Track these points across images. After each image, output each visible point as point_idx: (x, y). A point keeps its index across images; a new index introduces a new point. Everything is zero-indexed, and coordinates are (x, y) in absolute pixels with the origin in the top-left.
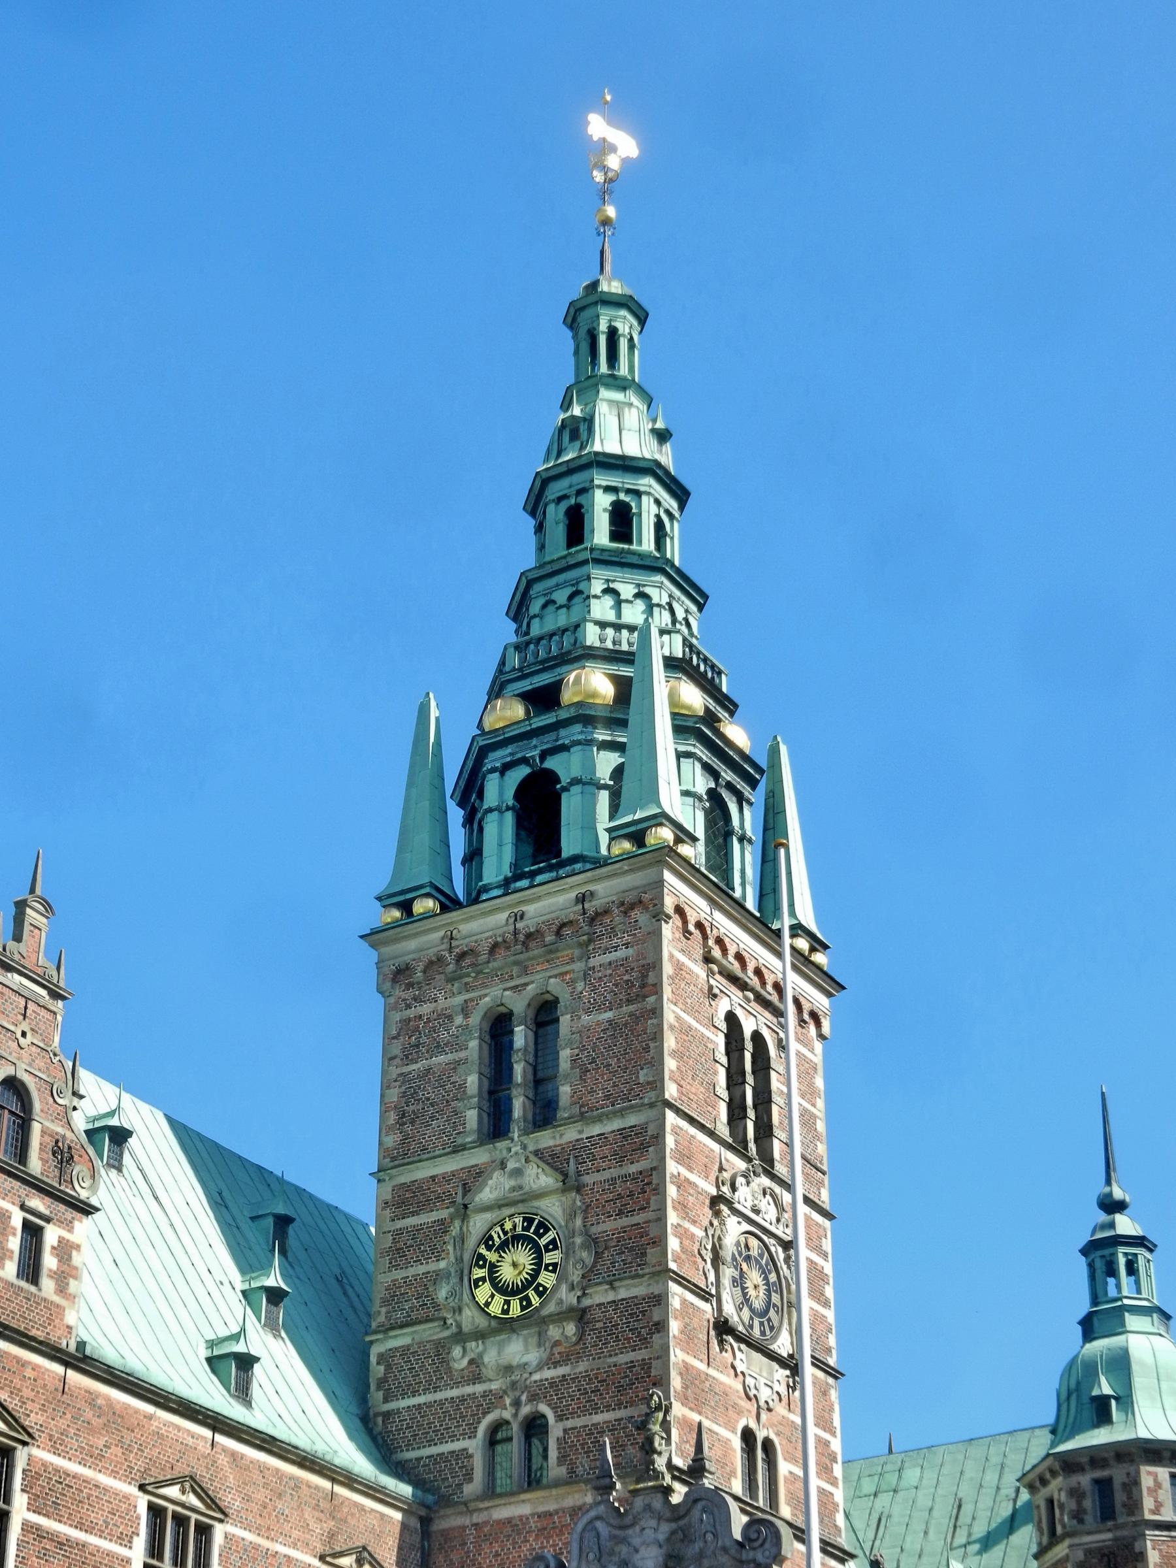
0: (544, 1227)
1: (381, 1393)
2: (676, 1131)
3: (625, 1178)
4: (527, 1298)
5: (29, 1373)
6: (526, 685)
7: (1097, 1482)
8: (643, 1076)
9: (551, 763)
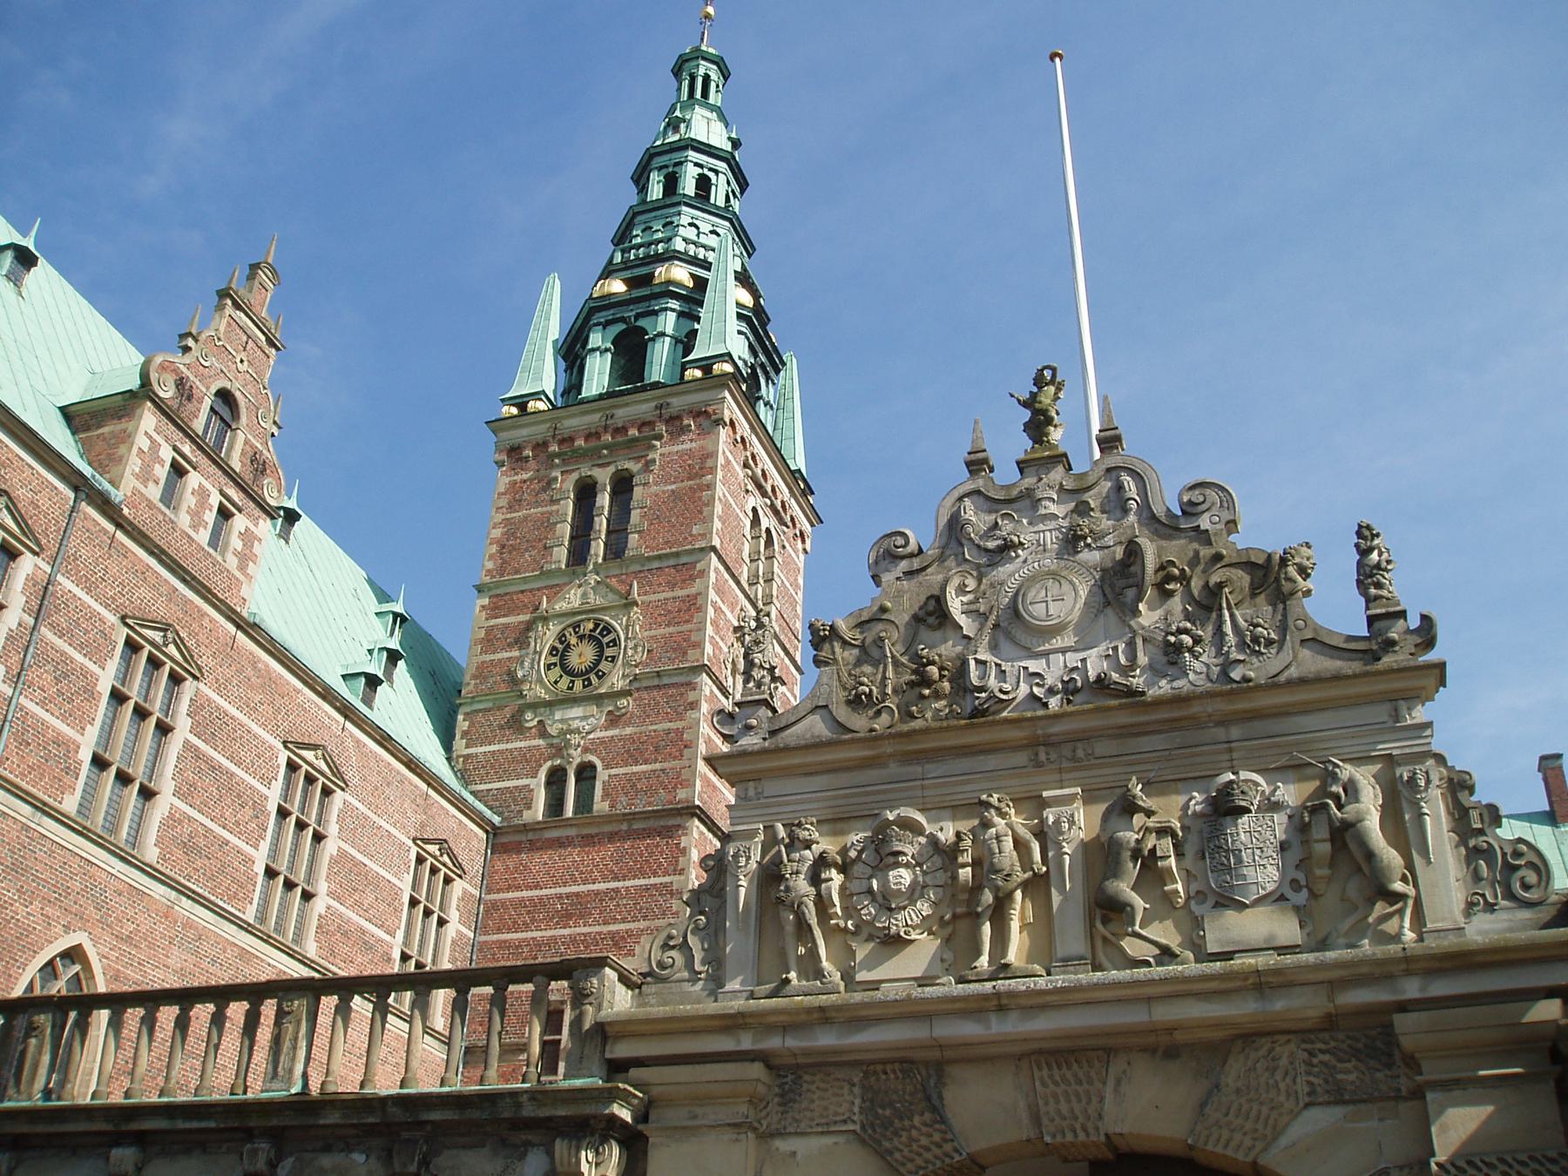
0: (608, 629)
2: (716, 569)
4: (589, 679)
5: (206, 622)
6: (628, 274)
9: (642, 323)
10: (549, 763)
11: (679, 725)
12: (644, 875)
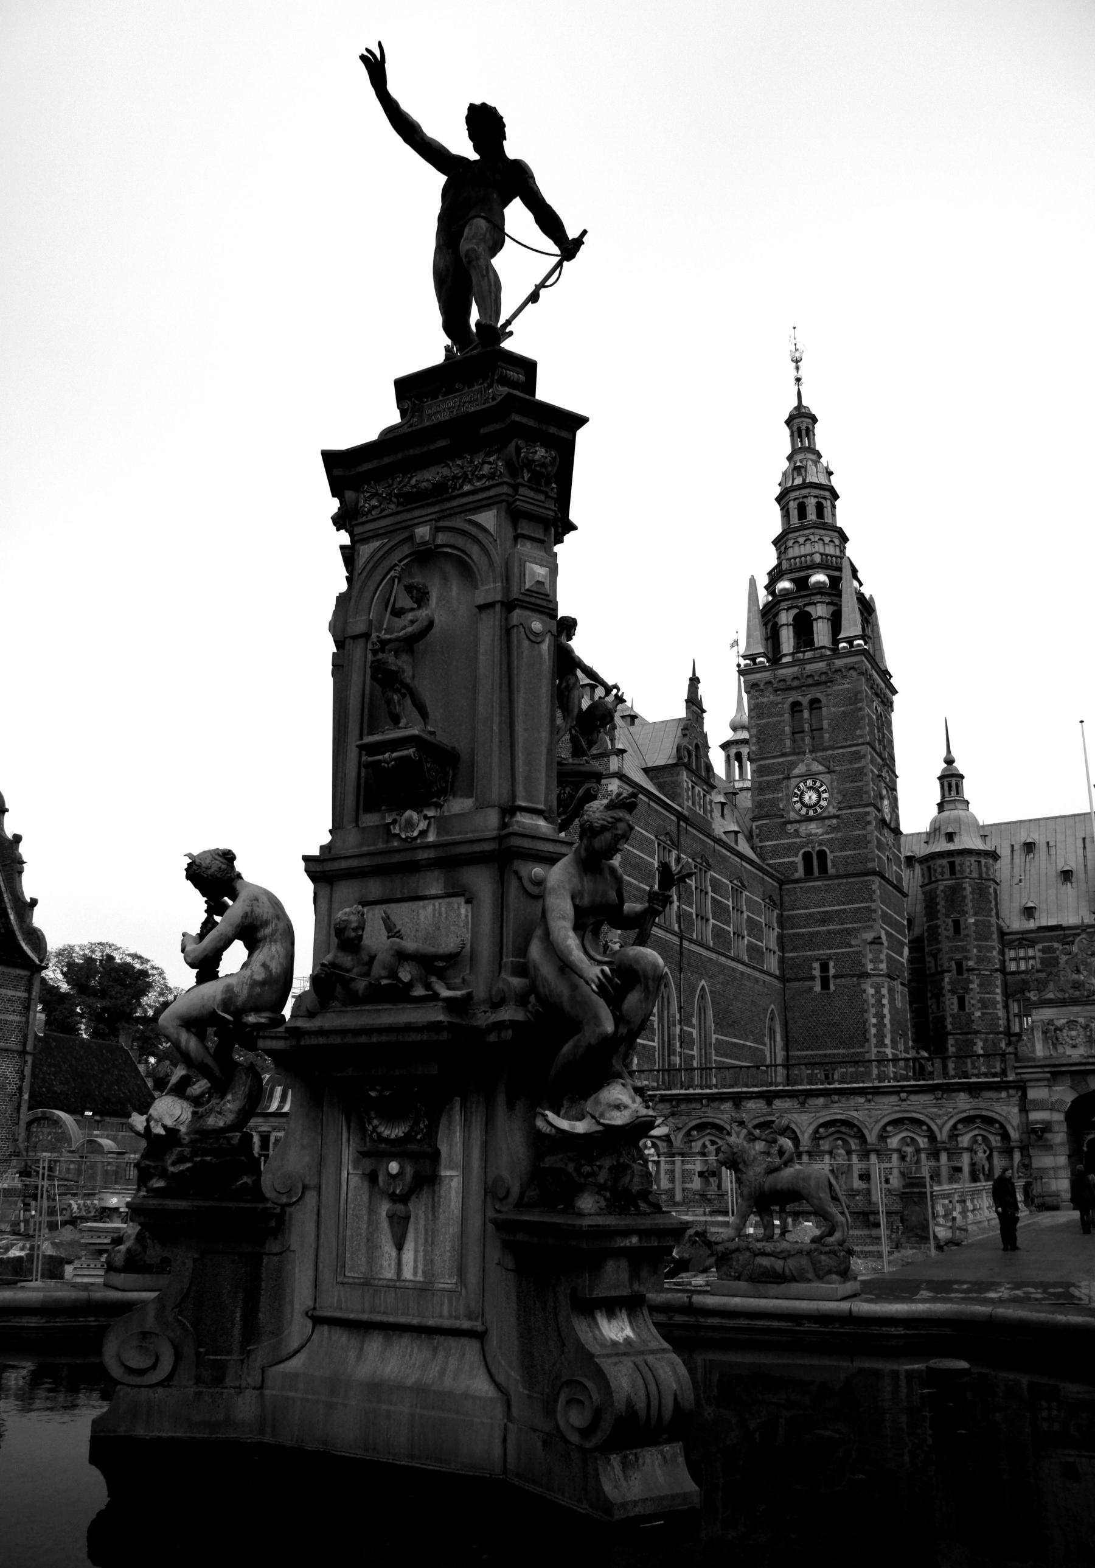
2: (870, 753)
3: (853, 769)
6: (793, 576)
7: (949, 862)
8: (858, 732)
9: (808, 609)
10: (803, 851)
11: (864, 832)
12: (857, 903)
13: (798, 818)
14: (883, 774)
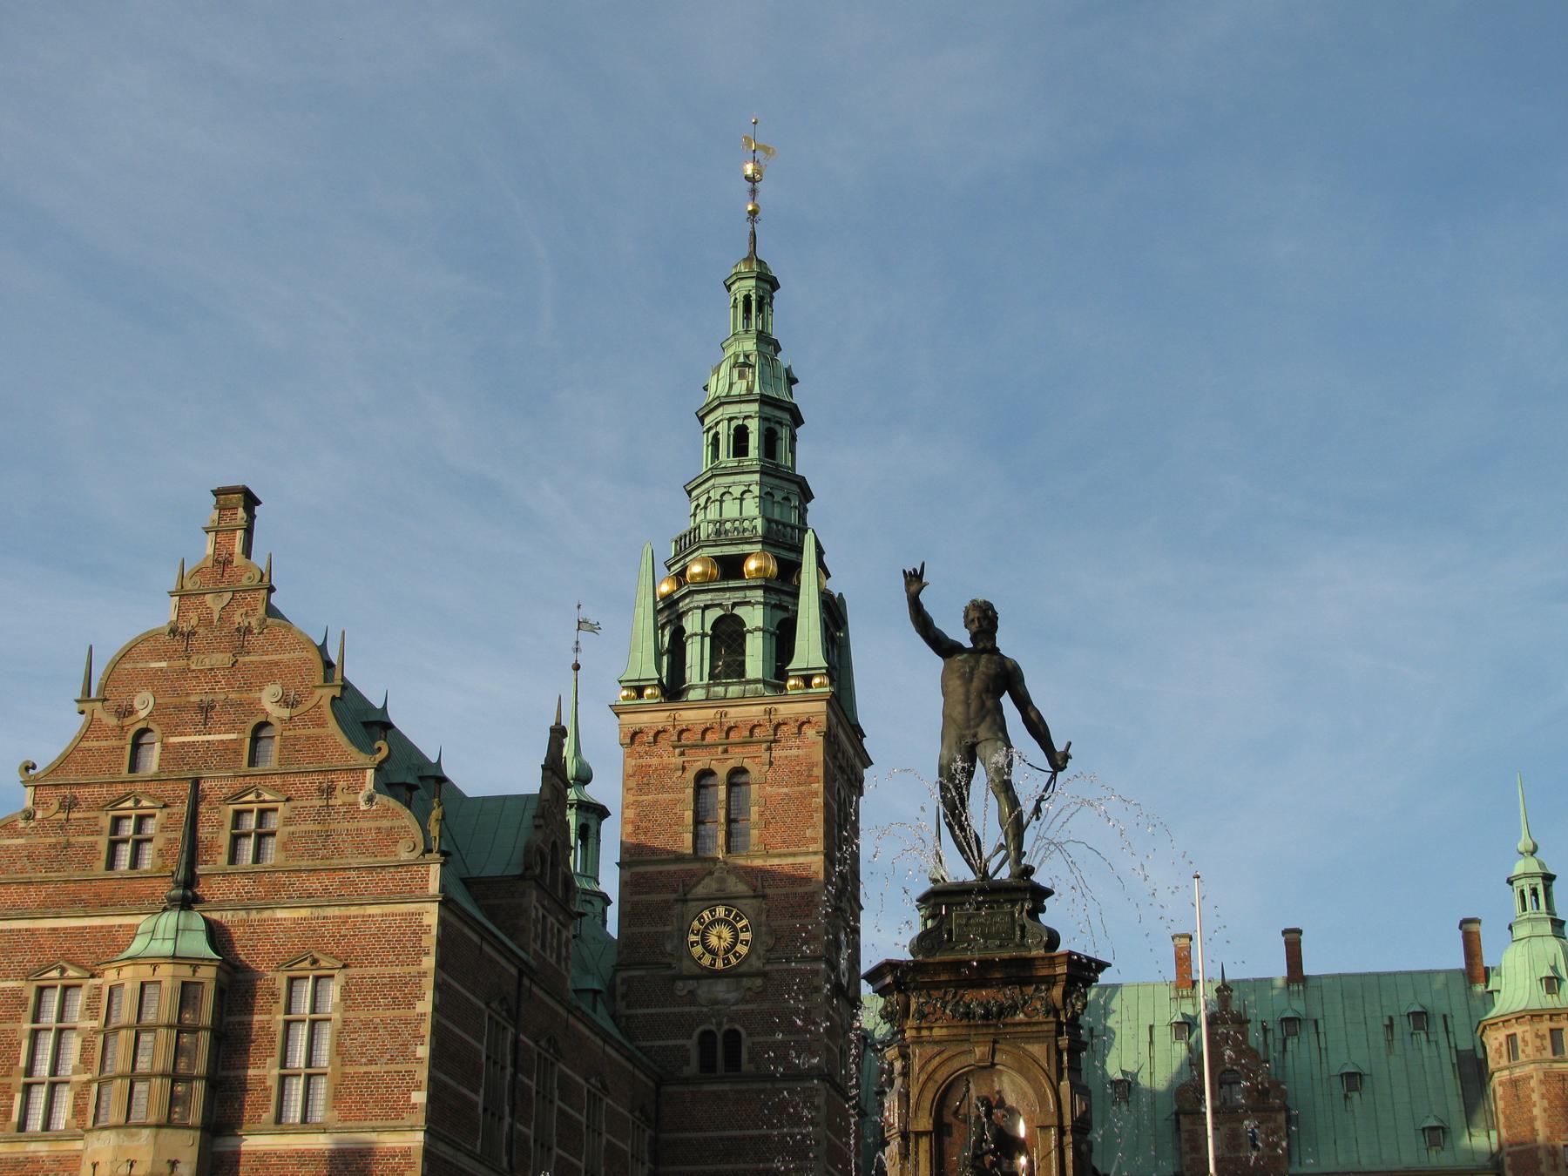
1: (624, 1003)
6: (717, 551)
8: (809, 833)
9: (738, 611)
10: (700, 1029)
13: (697, 971)
14: (842, 905)
